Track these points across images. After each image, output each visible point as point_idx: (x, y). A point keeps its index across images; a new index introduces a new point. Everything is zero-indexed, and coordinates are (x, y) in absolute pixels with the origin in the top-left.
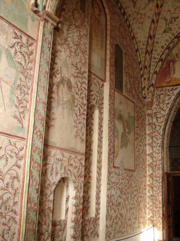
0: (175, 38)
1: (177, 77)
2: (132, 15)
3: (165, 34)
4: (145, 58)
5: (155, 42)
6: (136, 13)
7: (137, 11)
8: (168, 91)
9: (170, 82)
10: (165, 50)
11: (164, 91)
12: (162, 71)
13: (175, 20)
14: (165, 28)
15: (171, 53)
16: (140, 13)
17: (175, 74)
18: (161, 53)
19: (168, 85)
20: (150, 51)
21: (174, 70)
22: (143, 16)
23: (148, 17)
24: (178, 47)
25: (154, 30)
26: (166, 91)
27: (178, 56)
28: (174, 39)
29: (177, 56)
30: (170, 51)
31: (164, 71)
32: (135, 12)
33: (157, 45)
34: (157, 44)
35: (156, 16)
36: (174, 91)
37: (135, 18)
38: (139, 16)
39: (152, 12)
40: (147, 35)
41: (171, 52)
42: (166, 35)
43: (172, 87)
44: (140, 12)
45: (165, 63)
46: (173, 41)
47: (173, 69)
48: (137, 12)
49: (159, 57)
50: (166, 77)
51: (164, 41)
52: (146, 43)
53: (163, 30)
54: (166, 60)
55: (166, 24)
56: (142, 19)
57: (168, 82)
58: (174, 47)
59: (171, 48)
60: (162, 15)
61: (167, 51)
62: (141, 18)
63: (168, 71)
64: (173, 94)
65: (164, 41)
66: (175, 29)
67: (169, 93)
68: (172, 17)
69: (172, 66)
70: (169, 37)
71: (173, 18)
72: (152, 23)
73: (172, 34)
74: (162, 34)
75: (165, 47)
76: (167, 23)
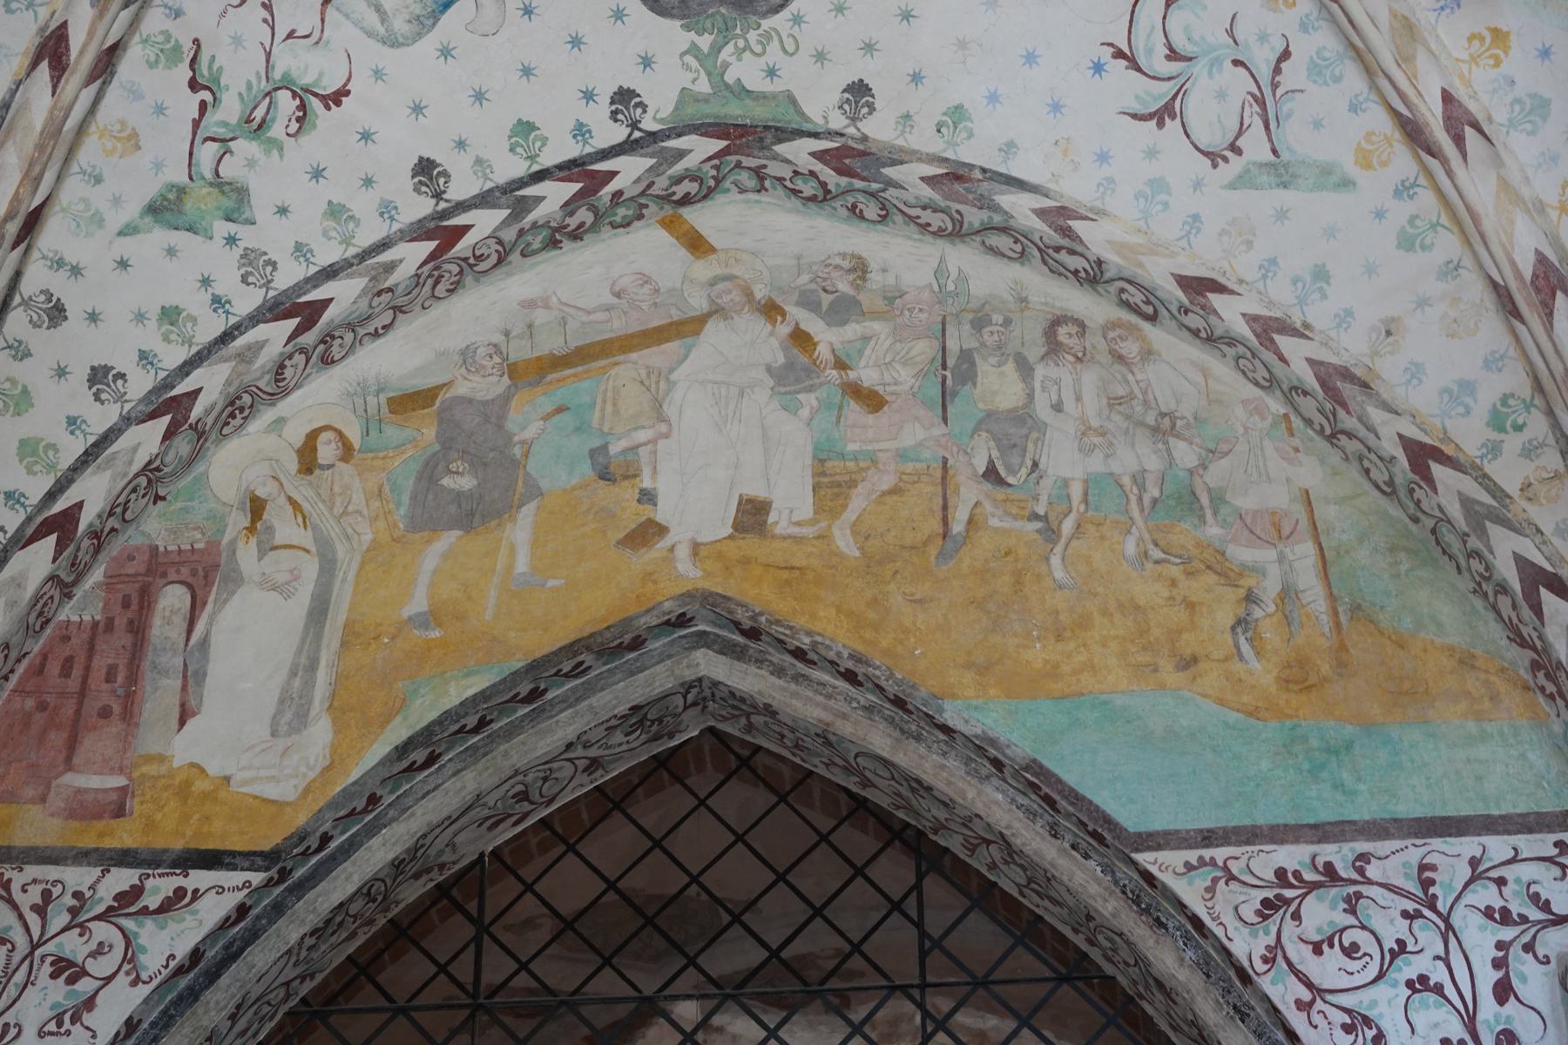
0: (275, 310)
1: (214, 768)
3: (160, 237)
5: (26, 303)
8: (74, 912)
9: (120, 812)
10: (127, 421)
11: (15, 907)
12: (44, 657)
15: (199, 468)
17: (191, 724)
18: (74, 448)
19: (88, 842)
21: (192, 677)
24: (281, 421)
25: (40, 147)
26: (40, 910)
27: (270, 530)
28: (255, 319)
29: (251, 529)
30: (183, 445)
31: (66, 672)
36: (149, 923)
41: (191, 462)
42: (171, 252)
43: (123, 879)
45: (97, 575)
46: (241, 342)
47: (178, 661)
49: (36, 488)
50: (72, 744)
51: (140, 317)
53: (150, 190)
54: (115, 548)
55: (196, 124)
57: (84, 809)
58: (237, 409)
59: (197, 412)
60: (178, 14)
61: (147, 439)
63: (110, 677)
64: (130, 958)
65: (140, 317)
66: (283, 211)
67: (73, 946)
68: (277, 75)
69: (176, 632)
70: (206, 282)
71: (286, 84)
72: (34, 64)
73: (248, 257)
74: (127, 231)
75: (139, 384)
76: (211, 118)
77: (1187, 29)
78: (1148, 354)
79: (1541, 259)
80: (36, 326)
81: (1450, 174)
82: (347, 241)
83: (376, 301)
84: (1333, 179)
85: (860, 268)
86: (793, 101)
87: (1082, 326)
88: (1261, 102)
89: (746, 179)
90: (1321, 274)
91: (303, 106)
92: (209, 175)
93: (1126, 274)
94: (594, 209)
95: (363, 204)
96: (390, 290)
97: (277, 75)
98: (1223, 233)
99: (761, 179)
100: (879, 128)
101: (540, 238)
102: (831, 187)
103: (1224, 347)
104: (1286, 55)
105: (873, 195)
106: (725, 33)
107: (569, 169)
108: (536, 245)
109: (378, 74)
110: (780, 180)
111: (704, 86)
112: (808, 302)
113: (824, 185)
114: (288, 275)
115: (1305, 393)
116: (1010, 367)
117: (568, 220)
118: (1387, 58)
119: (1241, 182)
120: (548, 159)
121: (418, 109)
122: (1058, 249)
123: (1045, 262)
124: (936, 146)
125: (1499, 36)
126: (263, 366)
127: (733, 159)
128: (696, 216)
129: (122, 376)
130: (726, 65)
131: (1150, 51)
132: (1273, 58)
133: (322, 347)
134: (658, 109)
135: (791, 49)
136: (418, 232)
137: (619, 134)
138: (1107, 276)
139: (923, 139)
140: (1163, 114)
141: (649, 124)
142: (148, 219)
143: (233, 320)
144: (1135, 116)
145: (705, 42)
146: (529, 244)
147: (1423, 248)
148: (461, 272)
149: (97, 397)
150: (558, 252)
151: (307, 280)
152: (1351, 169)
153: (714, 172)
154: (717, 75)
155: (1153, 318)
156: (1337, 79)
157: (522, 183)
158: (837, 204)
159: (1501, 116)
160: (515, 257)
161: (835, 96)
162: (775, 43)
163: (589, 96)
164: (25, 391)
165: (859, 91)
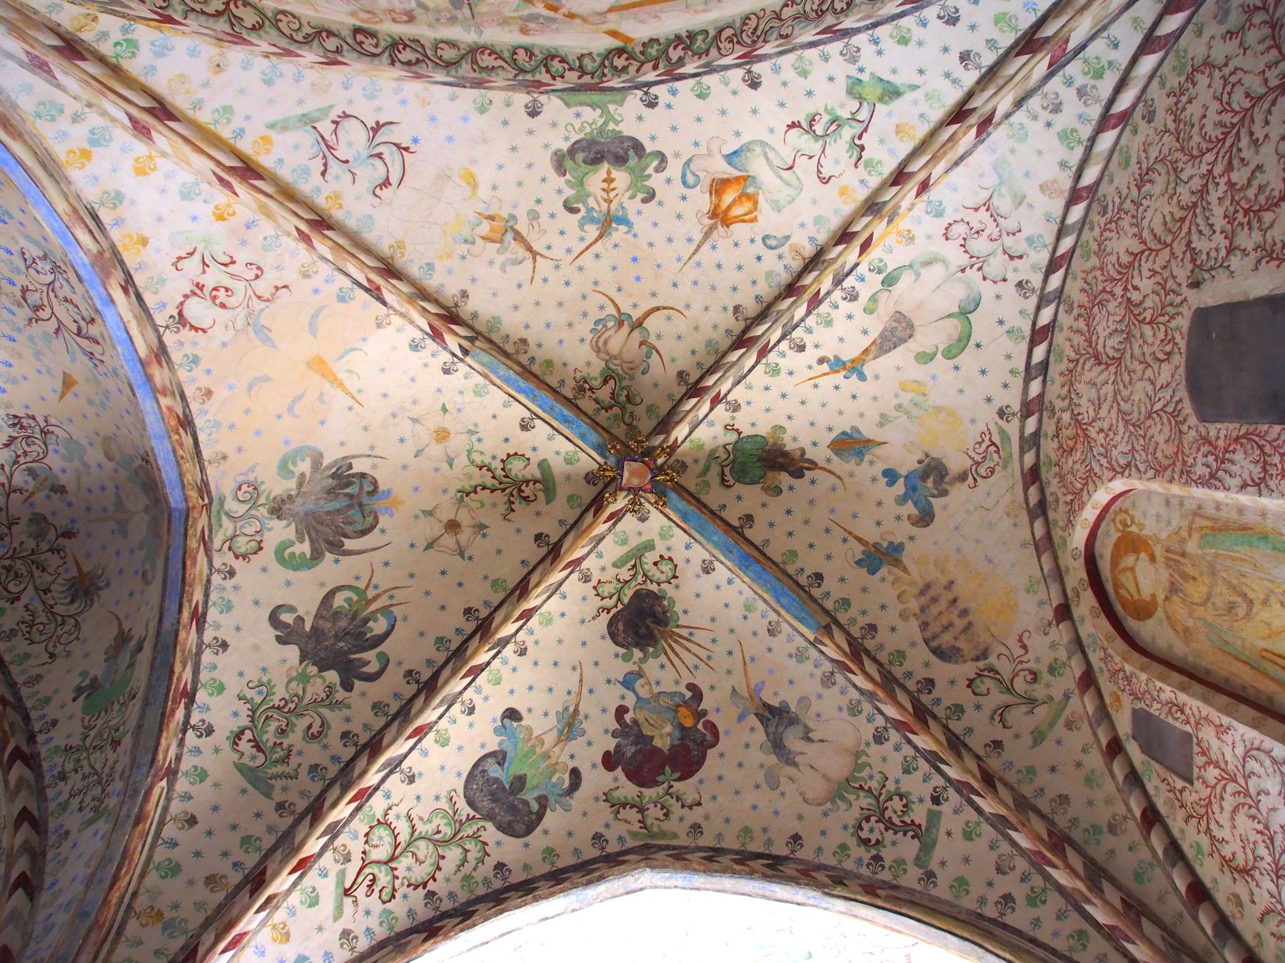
0: (847, 33)
2: (1013, 279)
3: (897, 80)
4: (1104, 28)
5: (979, 67)
6: (985, 267)
7: (973, 274)
13: (812, 122)
14: (880, 107)
16: (966, 252)
20: (1039, 56)
22: (960, 230)
23: (939, 214)
32: (984, 279)
33: (976, 43)
34: (975, 49)
35: (898, 206)
37: (1005, 252)
38: (980, 246)
39: (903, 223)
40: (998, 135)
42: (894, 71)
44: (964, 260)
48: (980, 269)
52: (1035, 103)
53: (897, 104)
55: (865, 130)
56: (977, 226)
60: (862, 181)
62: (978, 232)
66: (831, 79)
68: (821, 142)
71: (817, 137)
73: (854, 60)
74: (914, 87)
76: (858, 129)
77: (375, 169)
78: (353, 14)
79: (150, 139)
80: (978, 55)
81: (219, 163)
82: (800, 58)
83: (789, 31)
84: (282, 126)
85: (524, 31)
86: (568, 105)
87: (394, 20)
88: (329, 147)
89: (589, 65)
90: (268, 82)
91: (811, 126)
92: (865, 104)
93: (376, 61)
94: (669, 59)
95: (788, 73)
96: (781, 36)
97: (821, 142)
98: (330, 85)
99: (581, 67)
100: (522, 99)
101: (698, 44)
102: (543, 70)
103: (310, 31)
104: (323, 174)
105: (522, 71)
106: (601, 130)
107: (682, 77)
108: (700, 38)
109: (772, 131)
110: (571, 69)
111: (611, 107)
112: (553, 20)
113: (548, 71)
114: (835, 48)
115: (254, 28)
116: (431, 5)
117: (682, 54)
118: (271, 204)
119: (325, 111)
120: (691, 82)
121: (754, 112)
122: (418, 61)
123: (423, 47)
124: (491, 94)
125: (221, 218)
126: (859, 12)
127: (596, 80)
128: (615, 43)
129: (939, 17)
130: (601, 116)
131: (392, 154)
132: (329, 170)
133: (824, 8)
134: (634, 99)
135: (570, 128)
136: (762, 58)
137: (654, 90)
138: (386, 54)
139: (498, 97)
140: (377, 128)
141: (639, 93)
142: (902, 90)
143: (870, 32)
144: (392, 123)
145: (611, 126)
146: (704, 40)
147: (217, 110)
148: (742, 31)
149: (957, 11)
150: (690, 29)
151: (825, 43)
152: (273, 134)
153: (606, 71)
154: (604, 111)
155: (357, 31)
156: (294, 170)
157: (705, 73)
158: (540, 57)
159: (204, 186)
160: (712, 33)
161: (545, 109)
162: (577, 127)
163: (669, 106)
164: (996, 23)
165: (533, 113)
